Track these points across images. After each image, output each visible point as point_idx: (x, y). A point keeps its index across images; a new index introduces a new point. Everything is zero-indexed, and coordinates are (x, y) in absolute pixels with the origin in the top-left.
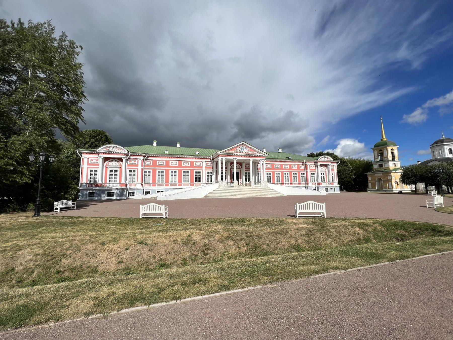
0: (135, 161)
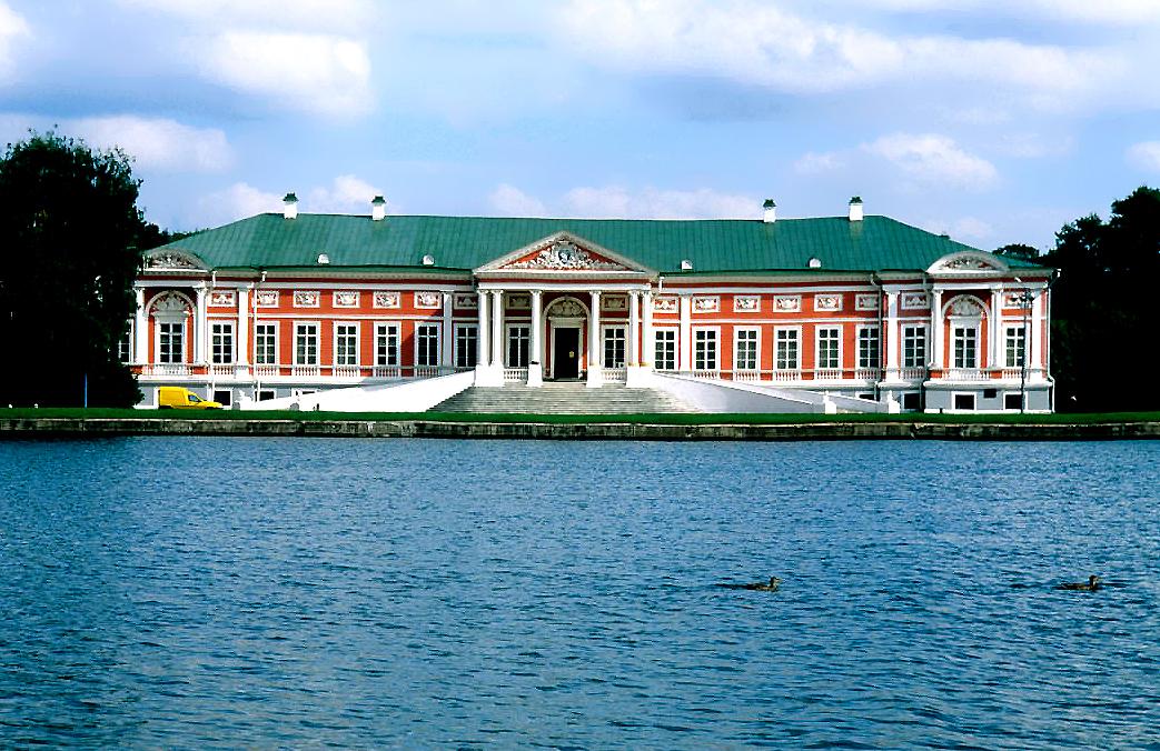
0: (229, 296)
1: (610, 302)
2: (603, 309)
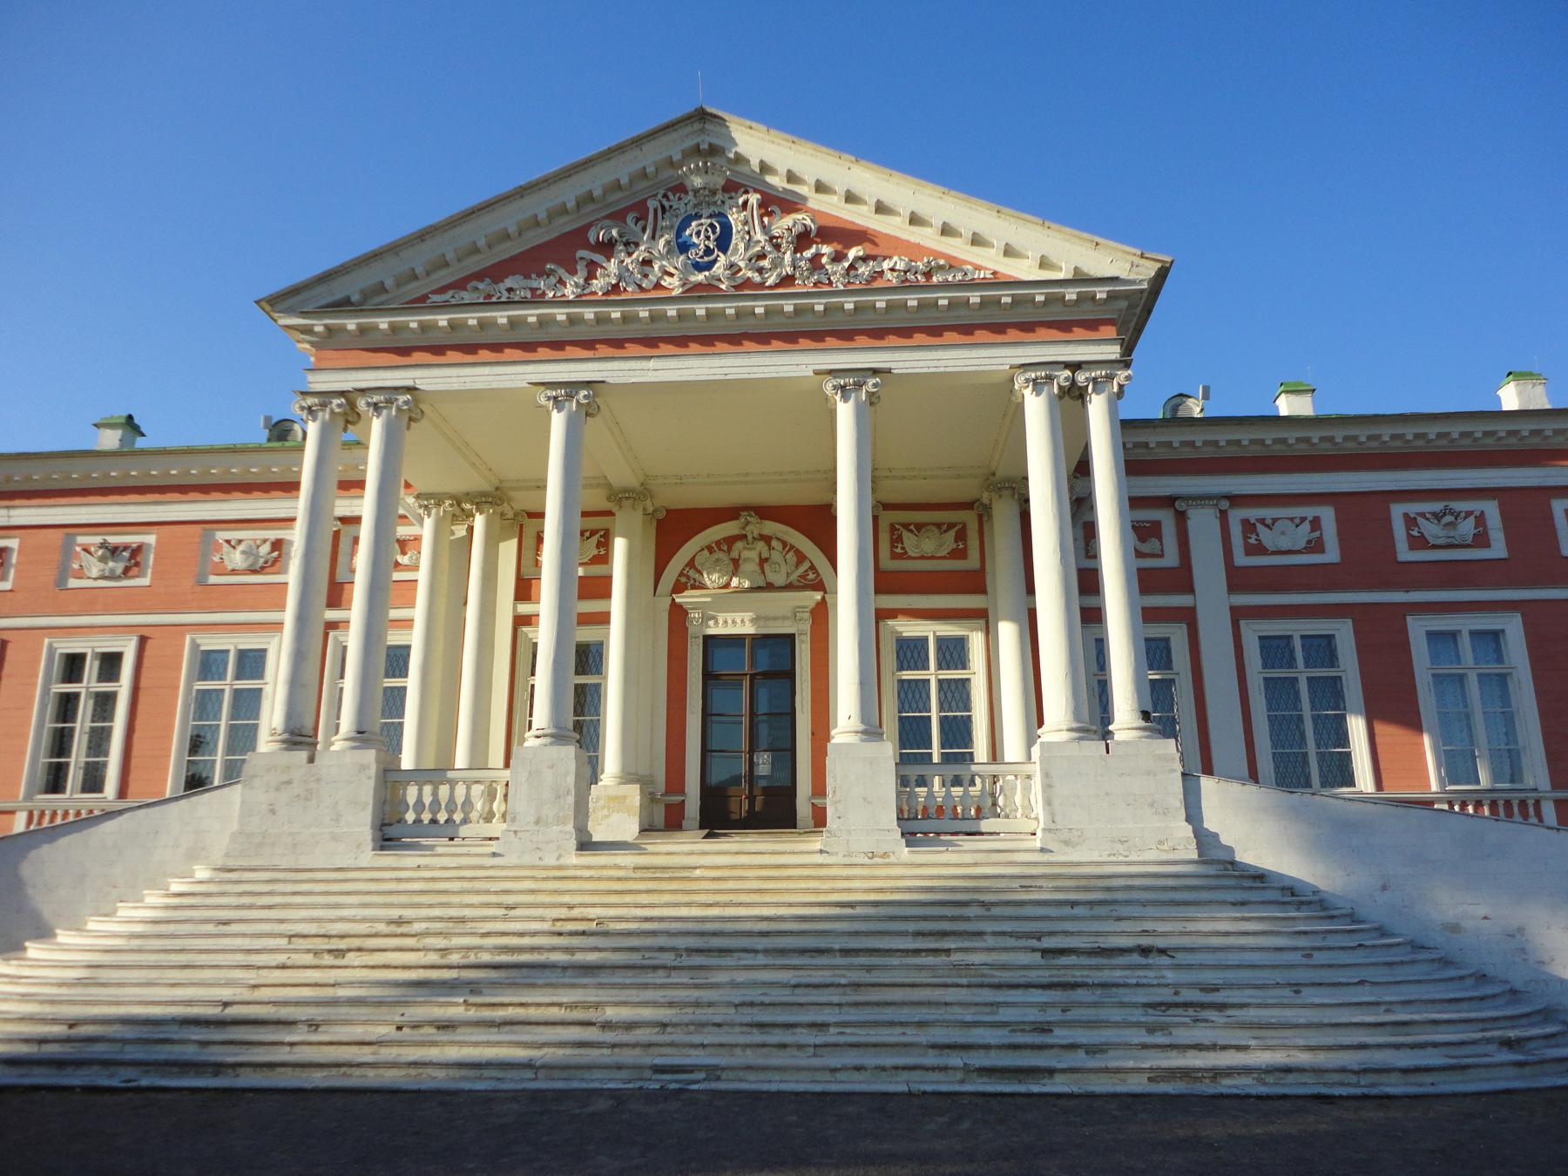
1: (909, 539)
2: (888, 564)
